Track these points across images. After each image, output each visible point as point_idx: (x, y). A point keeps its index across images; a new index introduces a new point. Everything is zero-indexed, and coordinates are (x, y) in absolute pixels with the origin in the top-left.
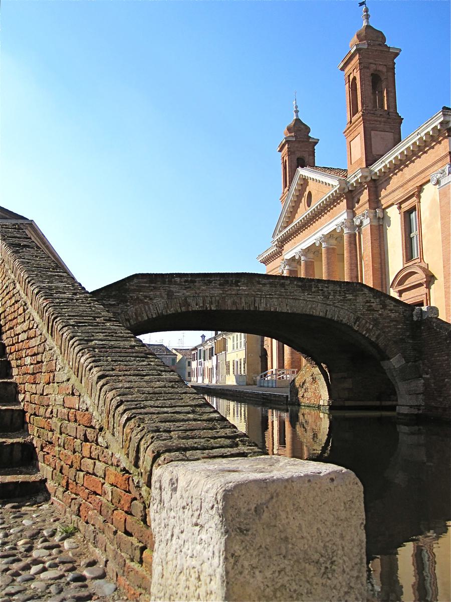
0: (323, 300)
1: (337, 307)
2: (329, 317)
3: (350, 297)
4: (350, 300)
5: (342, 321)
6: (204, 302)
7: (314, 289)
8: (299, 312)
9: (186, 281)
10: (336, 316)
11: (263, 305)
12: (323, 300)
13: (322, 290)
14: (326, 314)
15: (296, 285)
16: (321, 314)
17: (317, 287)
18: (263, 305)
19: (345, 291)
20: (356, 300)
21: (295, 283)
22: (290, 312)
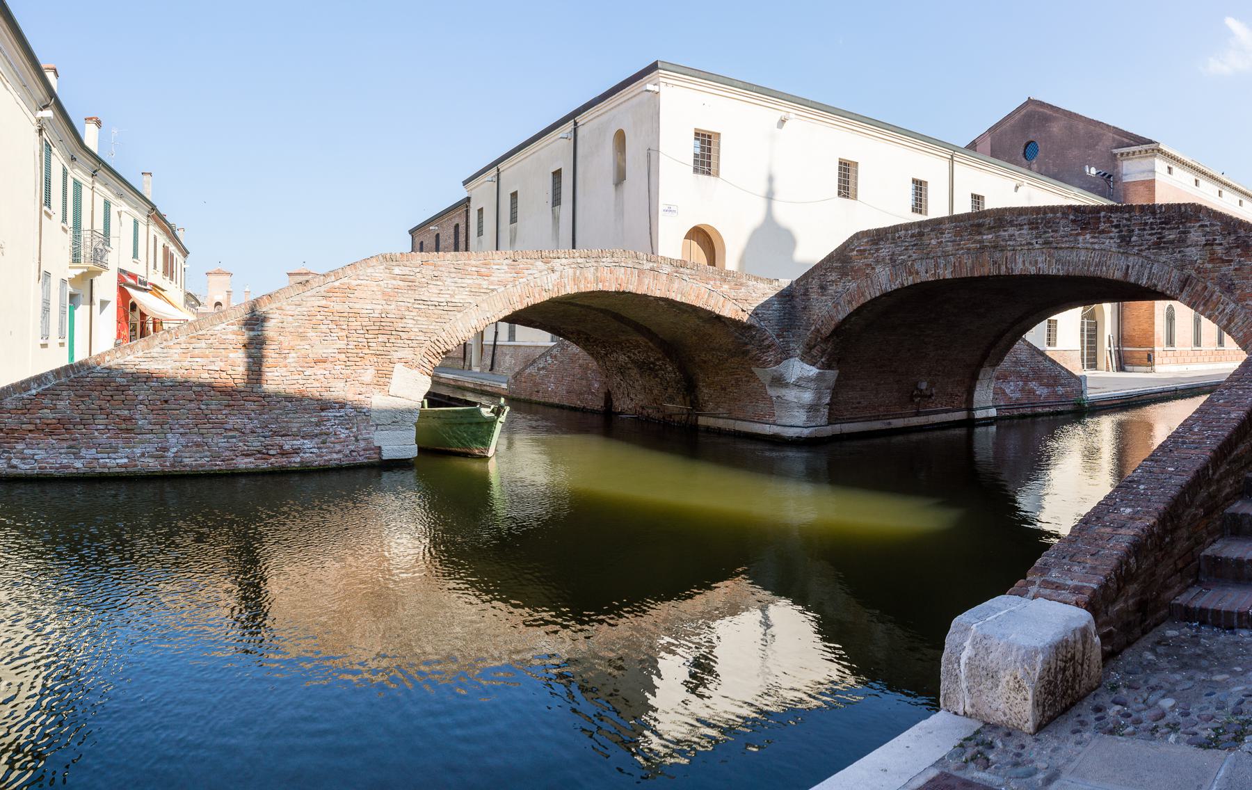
0: (1119, 247)
1: (1147, 258)
2: (1132, 280)
3: (1172, 236)
4: (1172, 242)
5: (1156, 286)
6: (936, 266)
7: (1102, 226)
8: (1077, 273)
9: (912, 236)
10: (1146, 274)
11: (1020, 266)
12: (1119, 247)
13: (1117, 226)
14: (1127, 273)
15: (1073, 221)
16: (1118, 275)
17: (1109, 220)
18: (1020, 266)
19: (1161, 223)
20: (1184, 241)
21: (1071, 217)
22: (1061, 273)
